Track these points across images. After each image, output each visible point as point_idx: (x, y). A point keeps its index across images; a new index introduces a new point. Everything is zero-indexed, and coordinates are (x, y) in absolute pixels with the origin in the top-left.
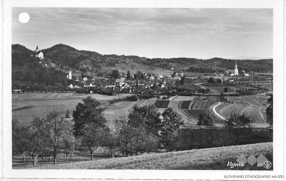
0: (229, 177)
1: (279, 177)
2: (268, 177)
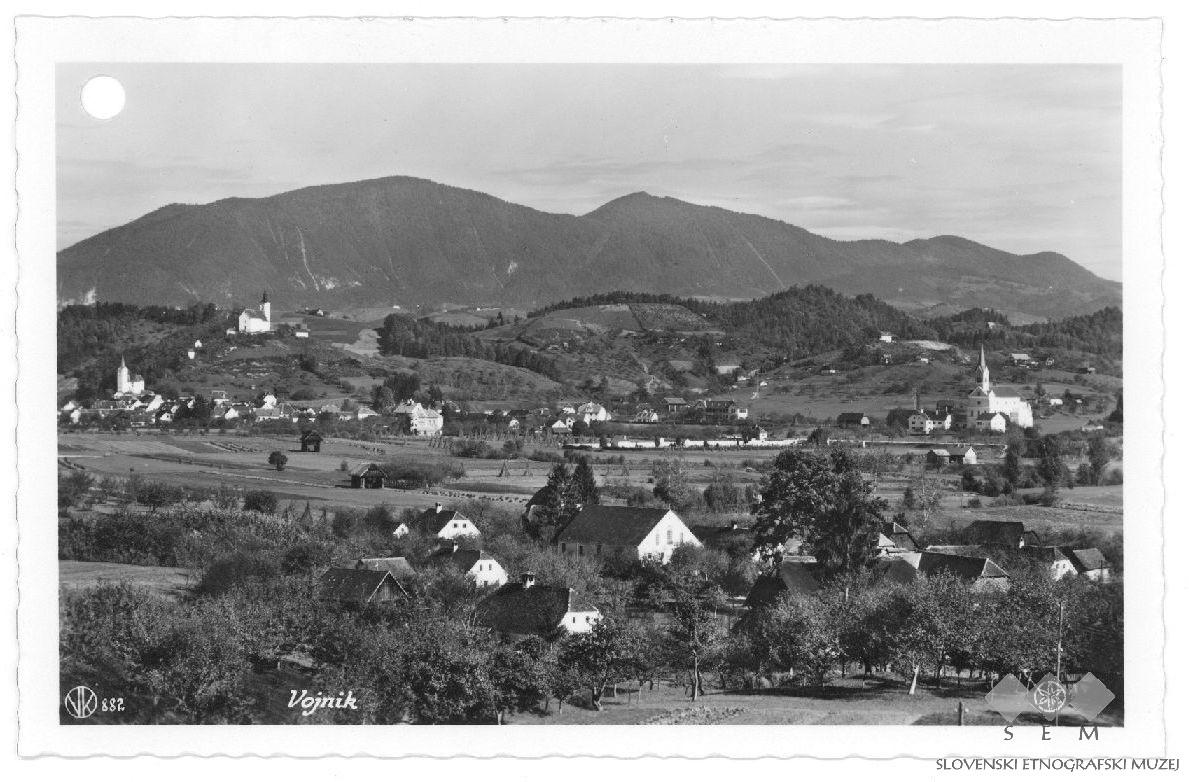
0: (957, 764)
1: (1158, 766)
2: (1115, 765)
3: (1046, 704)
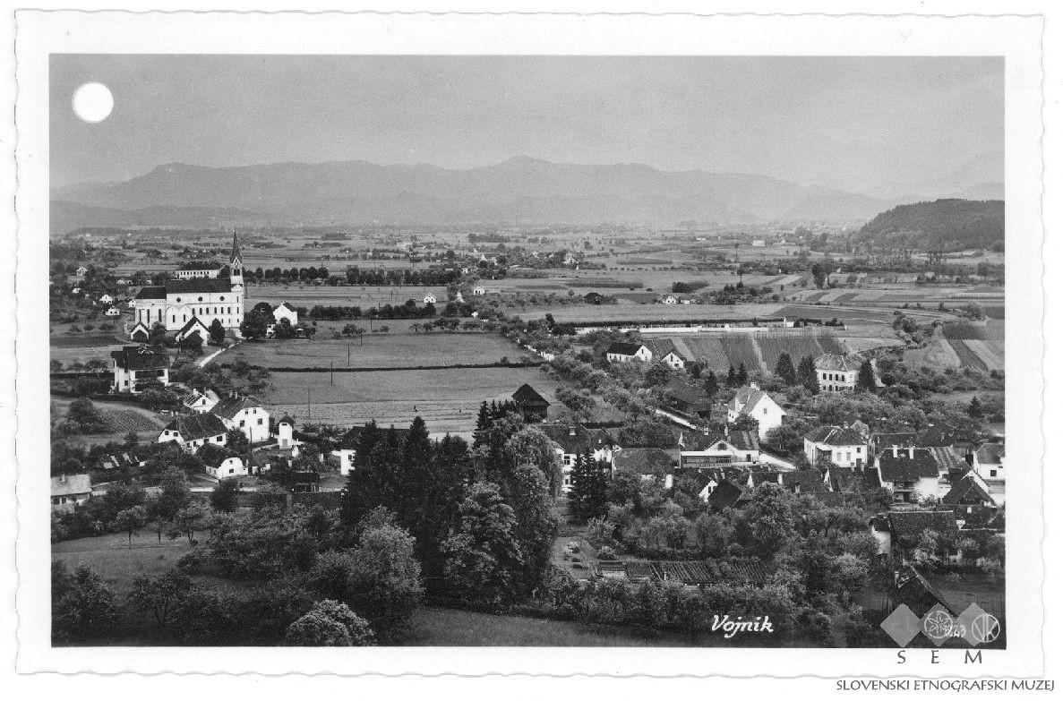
0: (856, 685)
2: (997, 686)
3: (935, 631)
